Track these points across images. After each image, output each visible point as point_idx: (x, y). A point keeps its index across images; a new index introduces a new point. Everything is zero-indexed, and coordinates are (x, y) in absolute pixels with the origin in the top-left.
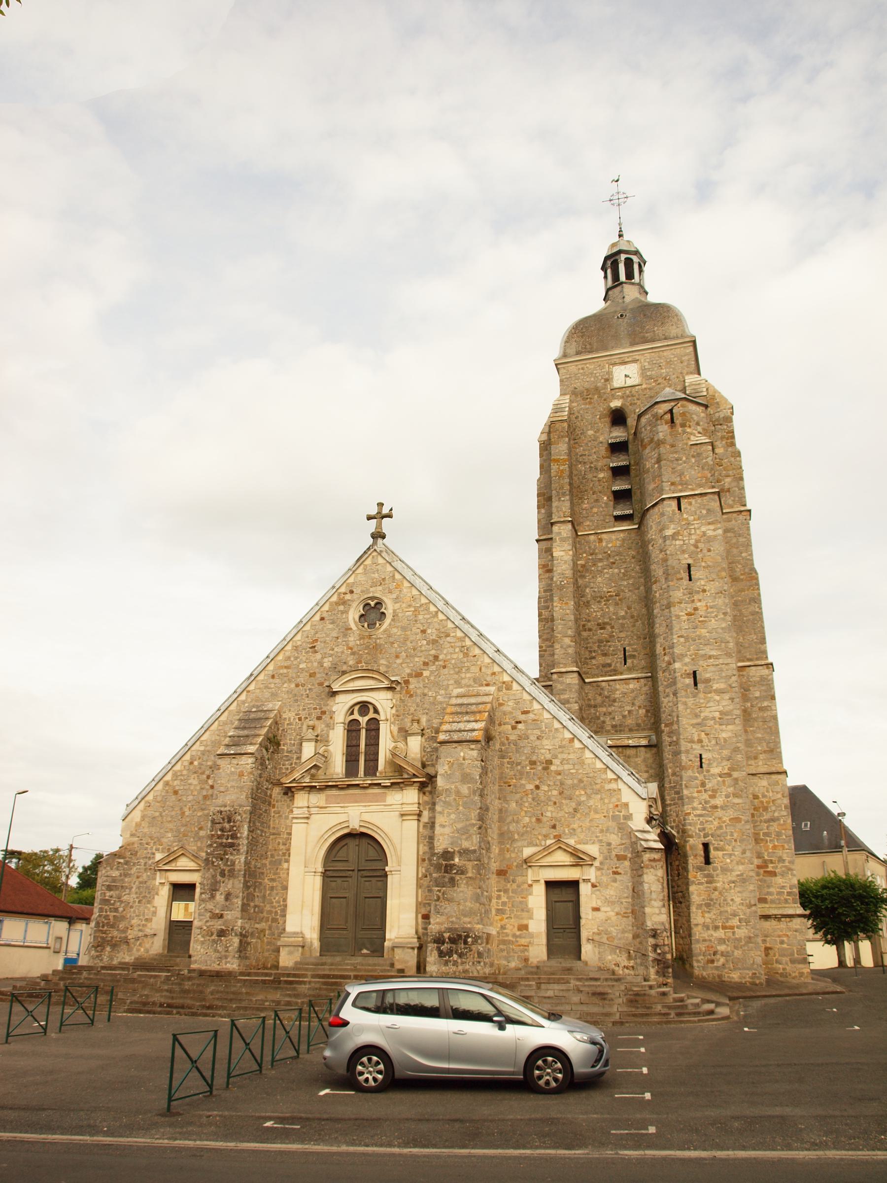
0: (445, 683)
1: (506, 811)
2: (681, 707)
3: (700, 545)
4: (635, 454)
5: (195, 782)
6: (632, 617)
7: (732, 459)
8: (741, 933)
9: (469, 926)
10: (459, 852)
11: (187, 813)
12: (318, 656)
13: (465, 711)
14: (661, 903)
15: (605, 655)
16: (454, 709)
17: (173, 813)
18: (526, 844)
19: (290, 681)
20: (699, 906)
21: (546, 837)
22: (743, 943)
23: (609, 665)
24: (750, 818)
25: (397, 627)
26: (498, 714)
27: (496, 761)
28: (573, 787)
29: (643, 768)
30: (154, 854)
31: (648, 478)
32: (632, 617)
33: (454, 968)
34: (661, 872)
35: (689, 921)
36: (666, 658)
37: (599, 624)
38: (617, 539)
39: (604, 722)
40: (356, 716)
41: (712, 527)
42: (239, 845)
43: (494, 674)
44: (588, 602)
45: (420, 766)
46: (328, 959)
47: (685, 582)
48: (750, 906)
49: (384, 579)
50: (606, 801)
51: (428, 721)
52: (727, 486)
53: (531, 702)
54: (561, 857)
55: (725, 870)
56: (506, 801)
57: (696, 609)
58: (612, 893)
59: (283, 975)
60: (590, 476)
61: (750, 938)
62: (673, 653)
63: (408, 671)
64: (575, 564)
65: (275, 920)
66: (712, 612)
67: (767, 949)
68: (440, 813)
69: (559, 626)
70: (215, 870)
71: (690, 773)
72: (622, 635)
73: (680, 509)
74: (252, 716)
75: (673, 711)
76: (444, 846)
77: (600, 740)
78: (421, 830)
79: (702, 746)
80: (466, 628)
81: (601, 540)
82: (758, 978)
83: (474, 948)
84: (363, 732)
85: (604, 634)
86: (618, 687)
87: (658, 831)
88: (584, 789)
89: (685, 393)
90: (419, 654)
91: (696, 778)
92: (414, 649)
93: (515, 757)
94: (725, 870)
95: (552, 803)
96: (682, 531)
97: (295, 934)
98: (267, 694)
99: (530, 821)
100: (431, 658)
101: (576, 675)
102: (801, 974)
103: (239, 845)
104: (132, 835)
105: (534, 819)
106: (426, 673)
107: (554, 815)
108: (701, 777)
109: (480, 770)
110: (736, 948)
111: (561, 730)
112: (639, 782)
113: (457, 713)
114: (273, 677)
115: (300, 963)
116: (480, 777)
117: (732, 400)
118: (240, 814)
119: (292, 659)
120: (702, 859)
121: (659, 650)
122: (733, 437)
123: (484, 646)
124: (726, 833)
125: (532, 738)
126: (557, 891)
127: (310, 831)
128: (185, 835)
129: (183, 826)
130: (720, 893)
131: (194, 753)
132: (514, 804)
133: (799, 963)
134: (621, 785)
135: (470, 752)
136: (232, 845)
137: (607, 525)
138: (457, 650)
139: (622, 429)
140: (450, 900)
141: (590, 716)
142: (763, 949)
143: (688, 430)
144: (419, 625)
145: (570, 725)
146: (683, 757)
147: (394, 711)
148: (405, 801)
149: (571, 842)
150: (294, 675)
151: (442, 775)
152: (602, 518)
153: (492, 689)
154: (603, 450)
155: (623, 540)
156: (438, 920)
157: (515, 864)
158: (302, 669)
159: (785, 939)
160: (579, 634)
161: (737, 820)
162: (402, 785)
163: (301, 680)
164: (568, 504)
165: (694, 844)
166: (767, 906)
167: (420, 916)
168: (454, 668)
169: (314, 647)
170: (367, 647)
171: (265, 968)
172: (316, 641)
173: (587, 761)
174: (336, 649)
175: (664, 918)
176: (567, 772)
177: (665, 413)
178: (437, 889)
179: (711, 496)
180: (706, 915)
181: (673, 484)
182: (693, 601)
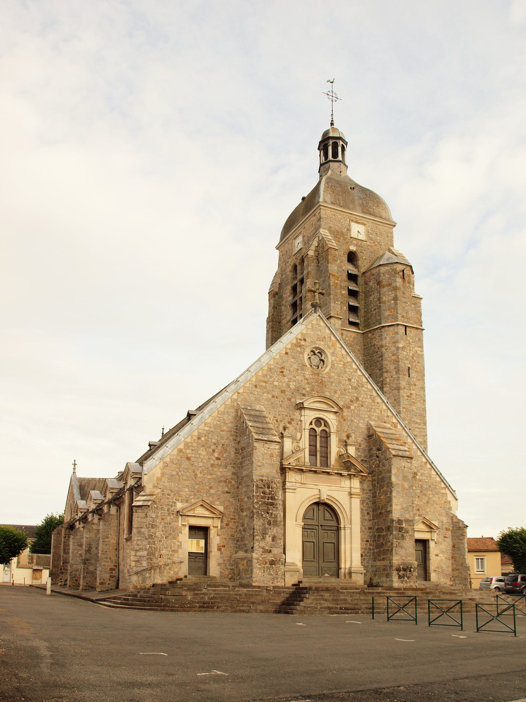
5: (204, 453)
11: (199, 475)
17: (188, 474)
19: (268, 393)
25: (334, 372)
28: (426, 489)
30: (175, 503)
40: (313, 426)
42: (277, 504)
43: (388, 416)
47: (407, 377)
57: (411, 394)
68: (395, 497)
83: (414, 573)
84: (318, 437)
90: (348, 394)
92: (345, 390)
95: (417, 497)
104: (154, 487)
118: (275, 483)
119: (268, 377)
128: (198, 491)
129: (196, 484)
131: (201, 431)
135: (407, 464)
136: (272, 504)
138: (369, 397)
140: (402, 547)
144: (347, 375)
150: (271, 389)
158: (276, 386)
163: (276, 393)
168: (367, 408)
169: (283, 372)
174: (297, 377)
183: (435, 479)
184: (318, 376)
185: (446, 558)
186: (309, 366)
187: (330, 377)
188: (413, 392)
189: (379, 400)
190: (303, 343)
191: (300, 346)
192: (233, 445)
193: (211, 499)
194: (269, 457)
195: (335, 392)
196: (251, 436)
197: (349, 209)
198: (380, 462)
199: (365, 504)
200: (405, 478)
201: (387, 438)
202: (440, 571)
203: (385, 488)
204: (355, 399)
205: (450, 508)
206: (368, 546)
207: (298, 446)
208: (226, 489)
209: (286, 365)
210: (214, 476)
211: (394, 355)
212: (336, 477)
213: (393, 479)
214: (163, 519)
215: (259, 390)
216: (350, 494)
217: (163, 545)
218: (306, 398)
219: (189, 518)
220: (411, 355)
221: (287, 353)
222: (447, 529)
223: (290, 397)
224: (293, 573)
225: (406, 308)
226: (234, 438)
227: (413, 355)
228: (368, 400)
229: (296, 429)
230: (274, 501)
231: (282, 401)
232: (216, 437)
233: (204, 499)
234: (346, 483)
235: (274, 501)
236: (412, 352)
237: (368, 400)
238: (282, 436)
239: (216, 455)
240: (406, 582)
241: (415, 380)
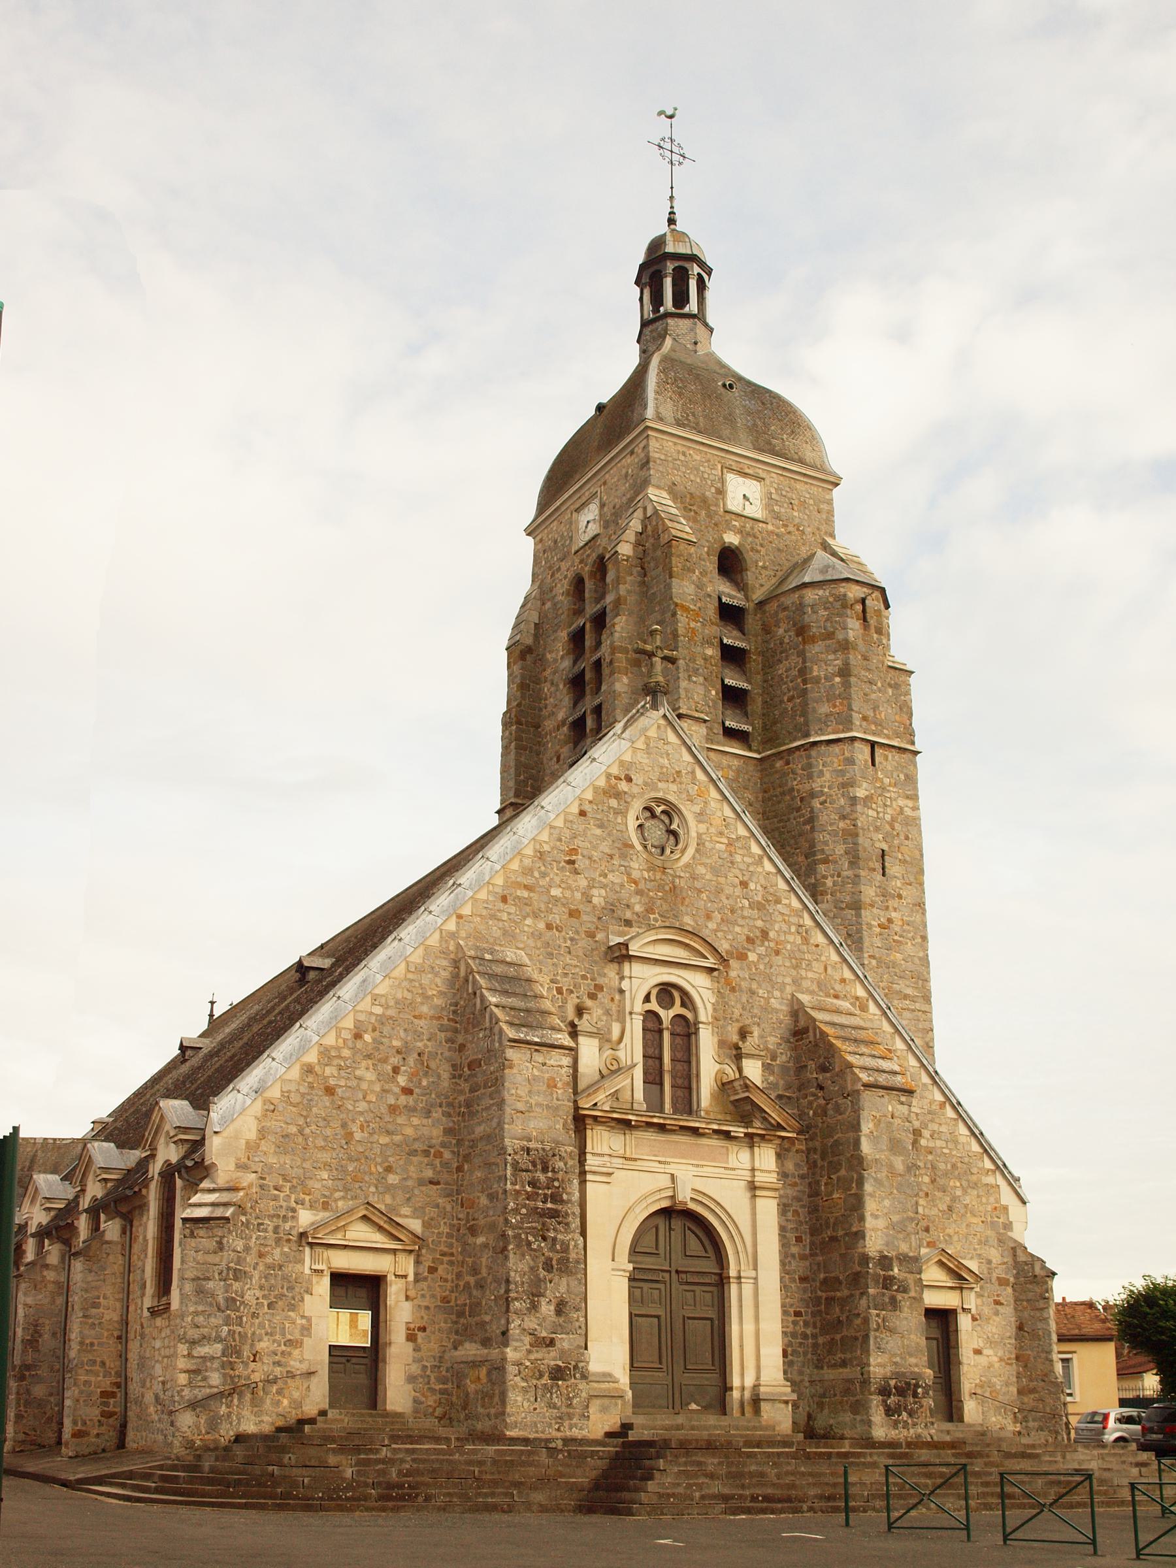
5: (370, 1076)
9: (916, 1370)
11: (358, 1136)
17: (328, 1132)
19: (536, 916)
28: (946, 1174)
30: (294, 1210)
40: (654, 1006)
42: (567, 1214)
43: (843, 981)
47: (879, 877)
57: (890, 921)
66: (909, 932)
68: (871, 1195)
83: (925, 1402)
84: (666, 1036)
90: (741, 922)
92: (733, 911)
106: (752, 957)
111: (930, 1087)
118: (561, 1158)
119: (536, 874)
128: (355, 1180)
129: (350, 1159)
131: (362, 1017)
135: (900, 1107)
136: (554, 1214)
138: (793, 929)
140: (892, 1331)
144: (737, 872)
150: (543, 906)
158: (557, 899)
163: (556, 919)
168: (790, 958)
169: (571, 862)
170: (660, 888)
172: (574, 851)
174: (610, 876)
176: (939, 1151)
184: (664, 873)
185: (1001, 1360)
186: (639, 848)
187: (694, 877)
188: (894, 915)
189: (820, 939)
190: (623, 786)
191: (618, 795)
192: (447, 1054)
193: (388, 1199)
194: (544, 1088)
195: (709, 917)
196: (496, 1030)
197: (720, 438)
198: (828, 1101)
199: (790, 1214)
200: (895, 1146)
201: (845, 1039)
202: (987, 1394)
203: (843, 1172)
204: (758, 934)
205: (1008, 1226)
206: (800, 1329)
207: (611, 1056)
208: (429, 1173)
209: (581, 844)
210: (398, 1138)
211: (843, 817)
212: (715, 1142)
213: (866, 1147)
215: (512, 910)
216: (753, 1187)
218: (634, 931)
220: (888, 818)
221: (583, 813)
222: (1002, 1282)
223: (593, 929)
224: (606, 1401)
225: (873, 696)
226: (449, 1034)
227: (893, 819)
228: (791, 938)
229: (607, 1012)
231: (572, 939)
232: (402, 1034)
233: (370, 1199)
234: (740, 1157)
236: (889, 810)
237: (791, 938)
238: (574, 1033)
239: (402, 1080)
240: (906, 1425)
241: (899, 884)
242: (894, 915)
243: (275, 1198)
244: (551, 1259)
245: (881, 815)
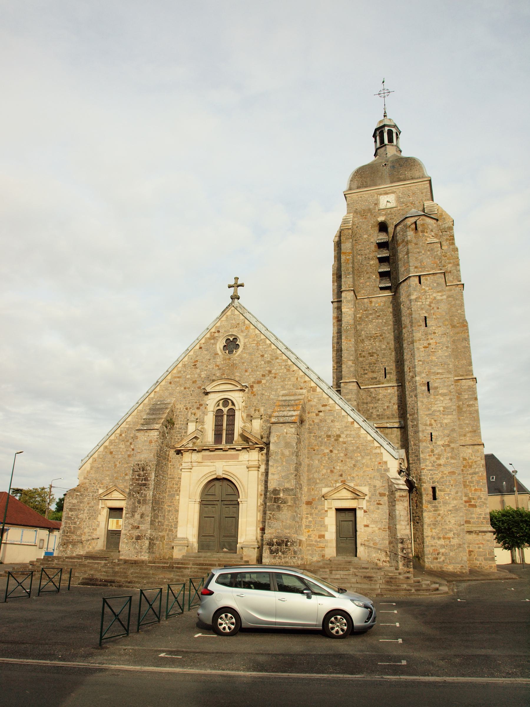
0: (275, 387)
1: (312, 466)
2: (419, 404)
3: (433, 305)
4: (393, 249)
6: (390, 349)
7: (453, 253)
8: (455, 541)
10: (283, 490)
11: (118, 466)
12: (198, 371)
13: (286, 404)
14: (406, 523)
15: (373, 372)
16: (281, 403)
18: (324, 485)
19: (181, 386)
20: (429, 525)
21: (336, 481)
22: (456, 548)
23: (376, 378)
24: (461, 472)
25: (246, 353)
26: (307, 407)
27: (306, 435)
28: (353, 451)
29: (396, 441)
31: (400, 264)
32: (390, 349)
33: (279, 561)
34: (406, 504)
35: (423, 534)
36: (411, 374)
37: (369, 353)
38: (381, 301)
39: (372, 413)
40: (221, 407)
41: (440, 294)
42: (149, 484)
44: (363, 340)
45: (260, 438)
46: (203, 554)
48: (460, 525)
49: (238, 324)
50: (373, 460)
51: (265, 410)
52: (449, 269)
53: (328, 399)
54: (345, 494)
55: (445, 503)
56: (312, 460)
58: (376, 516)
59: (175, 563)
60: (365, 263)
61: (460, 544)
62: (415, 371)
63: (253, 380)
64: (355, 316)
65: (171, 530)
67: (470, 552)
68: (272, 466)
69: (345, 354)
70: (134, 500)
71: (424, 444)
72: (384, 360)
73: (420, 283)
74: (158, 407)
75: (414, 407)
76: (274, 487)
77: (370, 423)
78: (260, 476)
79: (432, 428)
80: (288, 353)
81: (371, 302)
82: (465, 569)
83: (291, 548)
84: (225, 417)
85: (372, 359)
86: (381, 391)
87: (405, 479)
88: (360, 452)
89: (424, 212)
91: (428, 447)
92: (257, 367)
93: (318, 433)
94: (445, 503)
95: (340, 461)
96: (420, 296)
97: (183, 539)
98: (167, 394)
99: (327, 472)
100: (267, 372)
101: (355, 384)
102: (491, 567)
103: (149, 484)
105: (329, 471)
106: (263, 381)
107: (341, 468)
108: (431, 447)
109: (296, 441)
110: (451, 550)
112: (393, 448)
113: (283, 406)
114: (170, 383)
115: (186, 556)
116: (296, 444)
117: (453, 216)
118: (149, 466)
119: (182, 372)
120: (432, 497)
121: (406, 369)
122: (453, 239)
123: (299, 365)
124: (446, 480)
125: (329, 421)
126: (343, 514)
127: (192, 477)
130: (442, 517)
131: (122, 429)
132: (317, 462)
133: (490, 560)
134: (383, 450)
135: (290, 429)
136: (145, 485)
137: (375, 293)
138: (283, 367)
139: (385, 234)
141: (364, 408)
142: (467, 552)
143: (426, 234)
145: (351, 413)
146: (421, 434)
147: (244, 404)
148: (250, 459)
149: (352, 485)
151: (274, 443)
152: (372, 288)
153: (304, 391)
154: (373, 247)
155: (385, 302)
156: (270, 531)
157: (317, 498)
158: (188, 379)
159: (481, 546)
160: (357, 359)
161: (453, 473)
162: (248, 449)
163: (188, 385)
164: (351, 280)
165: (426, 487)
166: (470, 525)
167: (259, 529)
169: (196, 365)
170: (228, 365)
171: (164, 558)
172: (197, 361)
173: (362, 436)
174: (209, 366)
175: (408, 532)
177: (412, 224)
178: (269, 512)
179: (439, 275)
180: (433, 531)
181: (416, 267)
182: (428, 339)
183: (365, 439)
187: (241, 358)
190: (216, 335)
191: (214, 338)
205: (387, 470)
211: (408, 309)
214: (88, 504)
217: (86, 524)
219: (107, 501)
220: (428, 303)
222: (382, 495)
230: (147, 482)
231: (193, 391)
234: (244, 456)
235: (147, 482)
240: (280, 557)
242: (431, 341)
243: (93, 487)
244: (140, 500)
245: (424, 303)
